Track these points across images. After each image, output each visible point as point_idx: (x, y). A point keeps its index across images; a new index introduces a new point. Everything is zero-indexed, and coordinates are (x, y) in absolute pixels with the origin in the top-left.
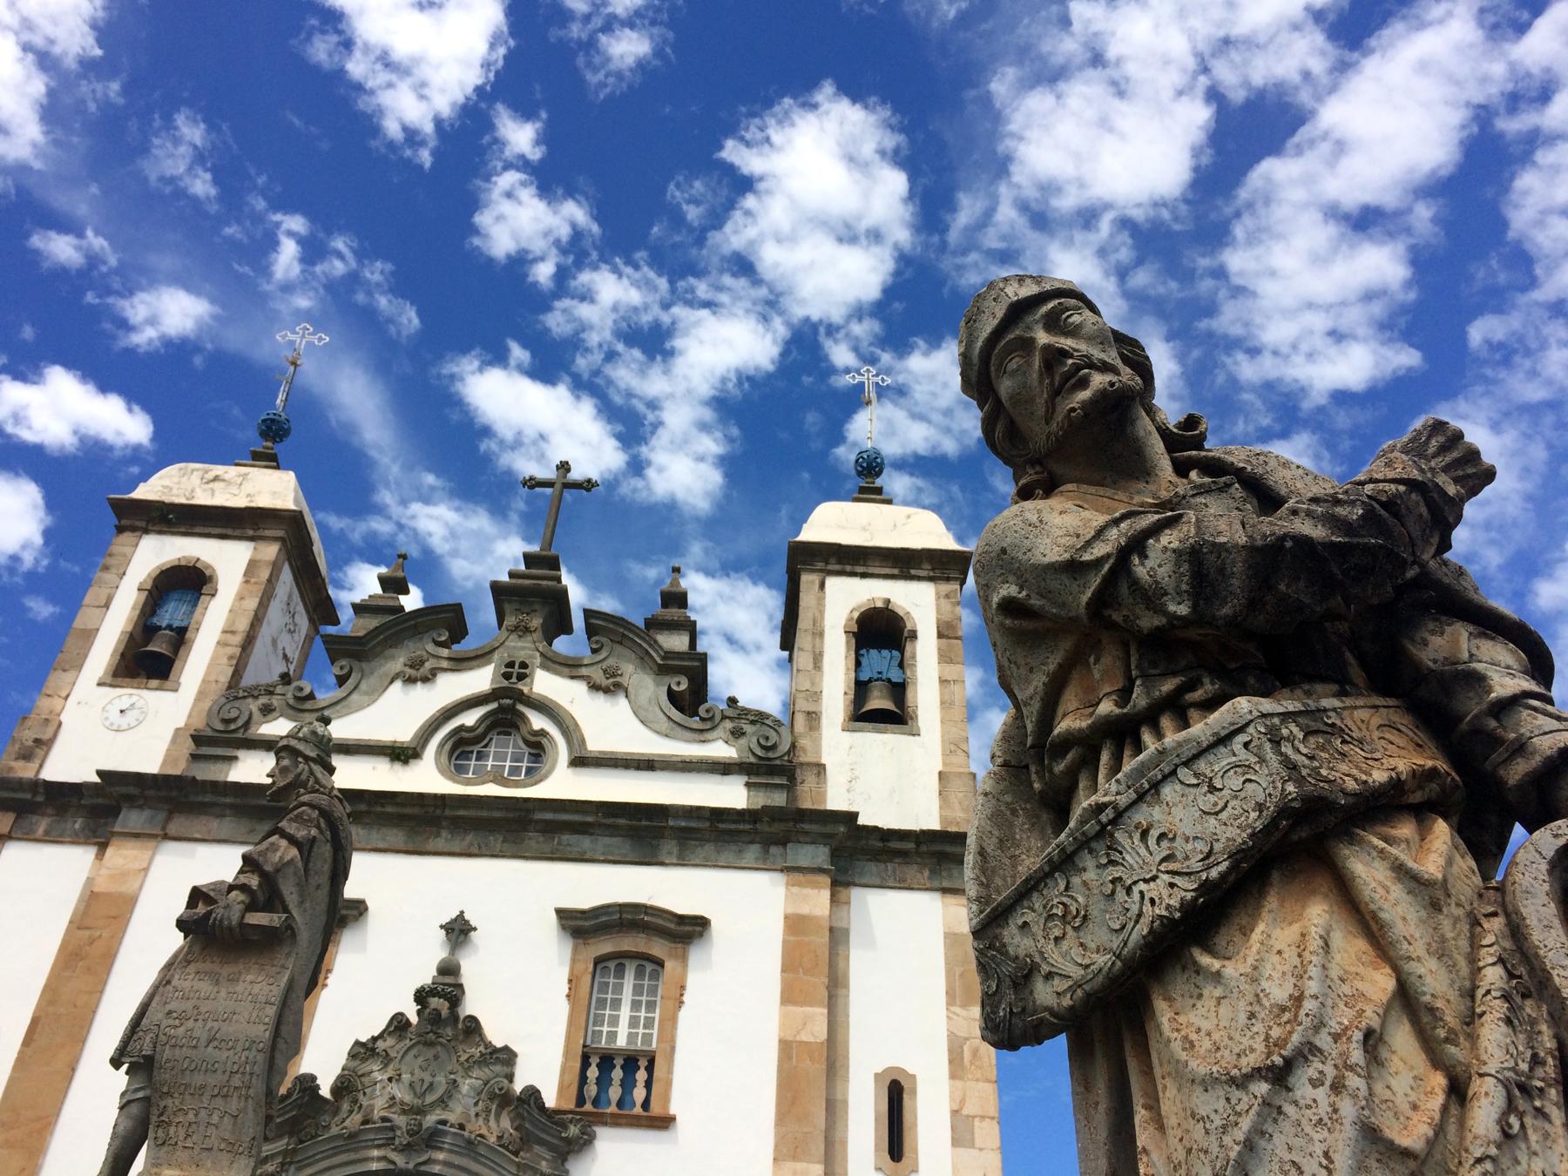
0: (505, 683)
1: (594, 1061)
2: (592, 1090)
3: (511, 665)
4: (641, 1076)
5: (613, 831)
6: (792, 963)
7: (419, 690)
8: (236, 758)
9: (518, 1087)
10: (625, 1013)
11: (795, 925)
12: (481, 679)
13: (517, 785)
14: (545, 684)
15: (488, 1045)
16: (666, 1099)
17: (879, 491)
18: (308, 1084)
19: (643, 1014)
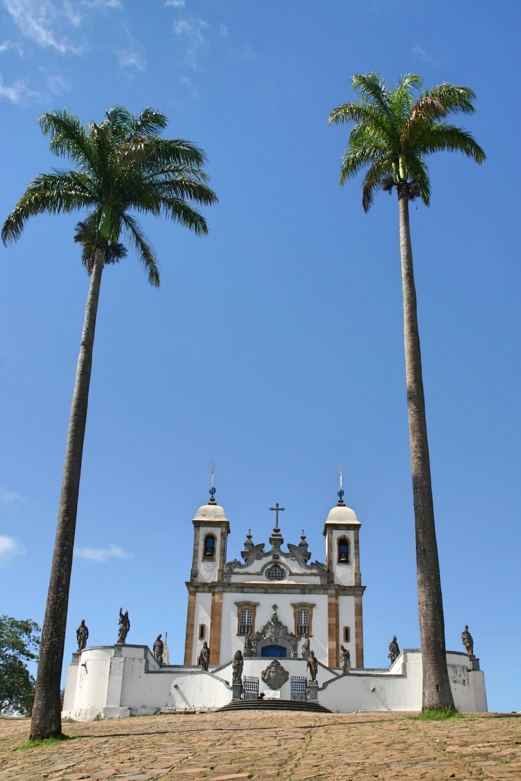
0: (274, 560)
1: (299, 627)
2: (299, 632)
3: (275, 555)
4: (307, 629)
5: (299, 589)
6: (329, 611)
7: (259, 561)
8: (231, 577)
9: (290, 633)
10: (303, 619)
11: (330, 604)
12: (270, 558)
13: (279, 580)
14: (283, 559)
15: (283, 626)
16: (311, 633)
17: (342, 501)
18: (258, 633)
19: (306, 619)
